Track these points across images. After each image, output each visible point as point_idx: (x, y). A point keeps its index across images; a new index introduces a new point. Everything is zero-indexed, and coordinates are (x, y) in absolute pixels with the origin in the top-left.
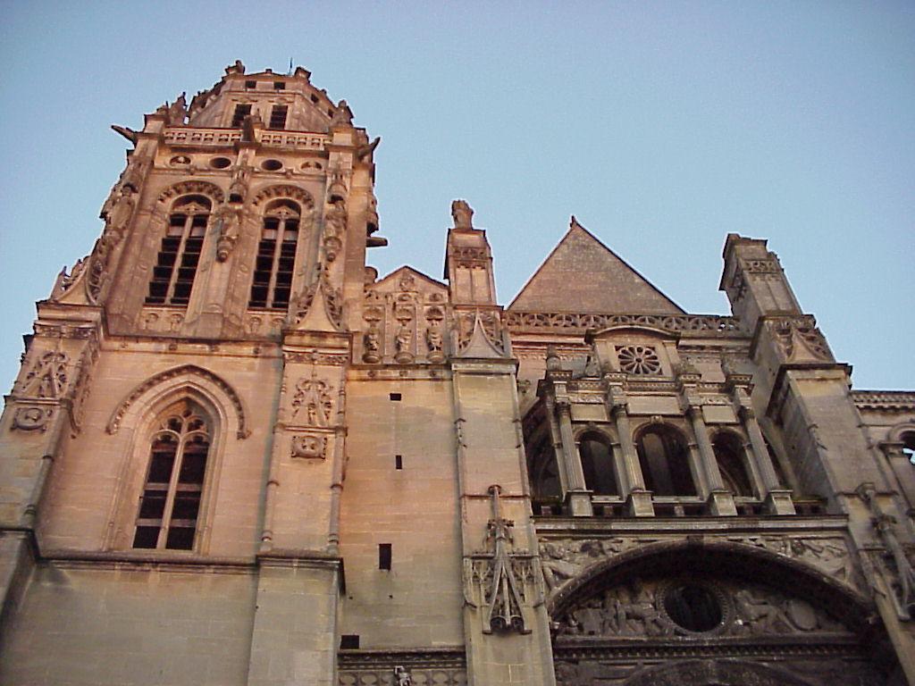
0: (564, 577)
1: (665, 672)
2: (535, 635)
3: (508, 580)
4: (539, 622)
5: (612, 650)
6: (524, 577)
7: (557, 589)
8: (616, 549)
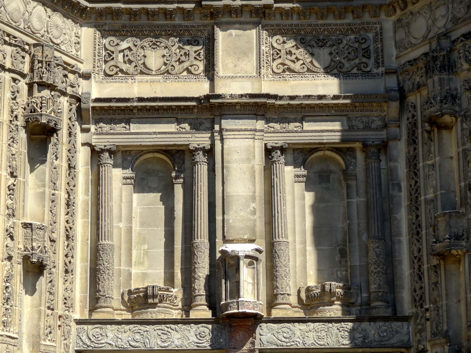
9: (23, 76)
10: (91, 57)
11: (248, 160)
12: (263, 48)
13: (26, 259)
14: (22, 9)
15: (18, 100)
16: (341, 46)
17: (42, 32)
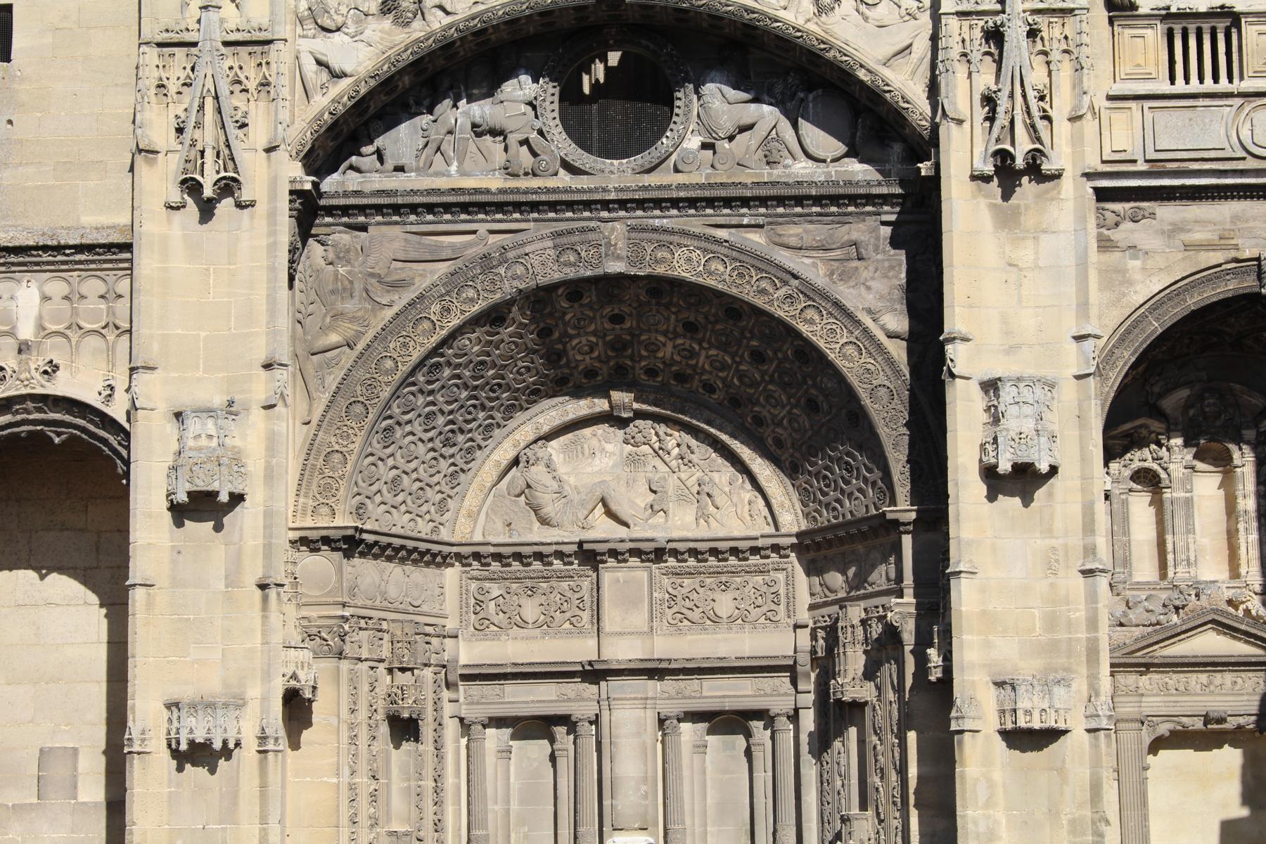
0: (337, 75)
1: (528, 249)
2: (261, 208)
3: (217, 98)
4: (273, 177)
5: (430, 208)
6: (252, 85)
7: (321, 102)
8: (449, 9)
10: (457, 610)
11: (639, 734)
12: (655, 595)
14: (377, 581)
15: (377, 690)
16: (746, 590)
17: (400, 599)
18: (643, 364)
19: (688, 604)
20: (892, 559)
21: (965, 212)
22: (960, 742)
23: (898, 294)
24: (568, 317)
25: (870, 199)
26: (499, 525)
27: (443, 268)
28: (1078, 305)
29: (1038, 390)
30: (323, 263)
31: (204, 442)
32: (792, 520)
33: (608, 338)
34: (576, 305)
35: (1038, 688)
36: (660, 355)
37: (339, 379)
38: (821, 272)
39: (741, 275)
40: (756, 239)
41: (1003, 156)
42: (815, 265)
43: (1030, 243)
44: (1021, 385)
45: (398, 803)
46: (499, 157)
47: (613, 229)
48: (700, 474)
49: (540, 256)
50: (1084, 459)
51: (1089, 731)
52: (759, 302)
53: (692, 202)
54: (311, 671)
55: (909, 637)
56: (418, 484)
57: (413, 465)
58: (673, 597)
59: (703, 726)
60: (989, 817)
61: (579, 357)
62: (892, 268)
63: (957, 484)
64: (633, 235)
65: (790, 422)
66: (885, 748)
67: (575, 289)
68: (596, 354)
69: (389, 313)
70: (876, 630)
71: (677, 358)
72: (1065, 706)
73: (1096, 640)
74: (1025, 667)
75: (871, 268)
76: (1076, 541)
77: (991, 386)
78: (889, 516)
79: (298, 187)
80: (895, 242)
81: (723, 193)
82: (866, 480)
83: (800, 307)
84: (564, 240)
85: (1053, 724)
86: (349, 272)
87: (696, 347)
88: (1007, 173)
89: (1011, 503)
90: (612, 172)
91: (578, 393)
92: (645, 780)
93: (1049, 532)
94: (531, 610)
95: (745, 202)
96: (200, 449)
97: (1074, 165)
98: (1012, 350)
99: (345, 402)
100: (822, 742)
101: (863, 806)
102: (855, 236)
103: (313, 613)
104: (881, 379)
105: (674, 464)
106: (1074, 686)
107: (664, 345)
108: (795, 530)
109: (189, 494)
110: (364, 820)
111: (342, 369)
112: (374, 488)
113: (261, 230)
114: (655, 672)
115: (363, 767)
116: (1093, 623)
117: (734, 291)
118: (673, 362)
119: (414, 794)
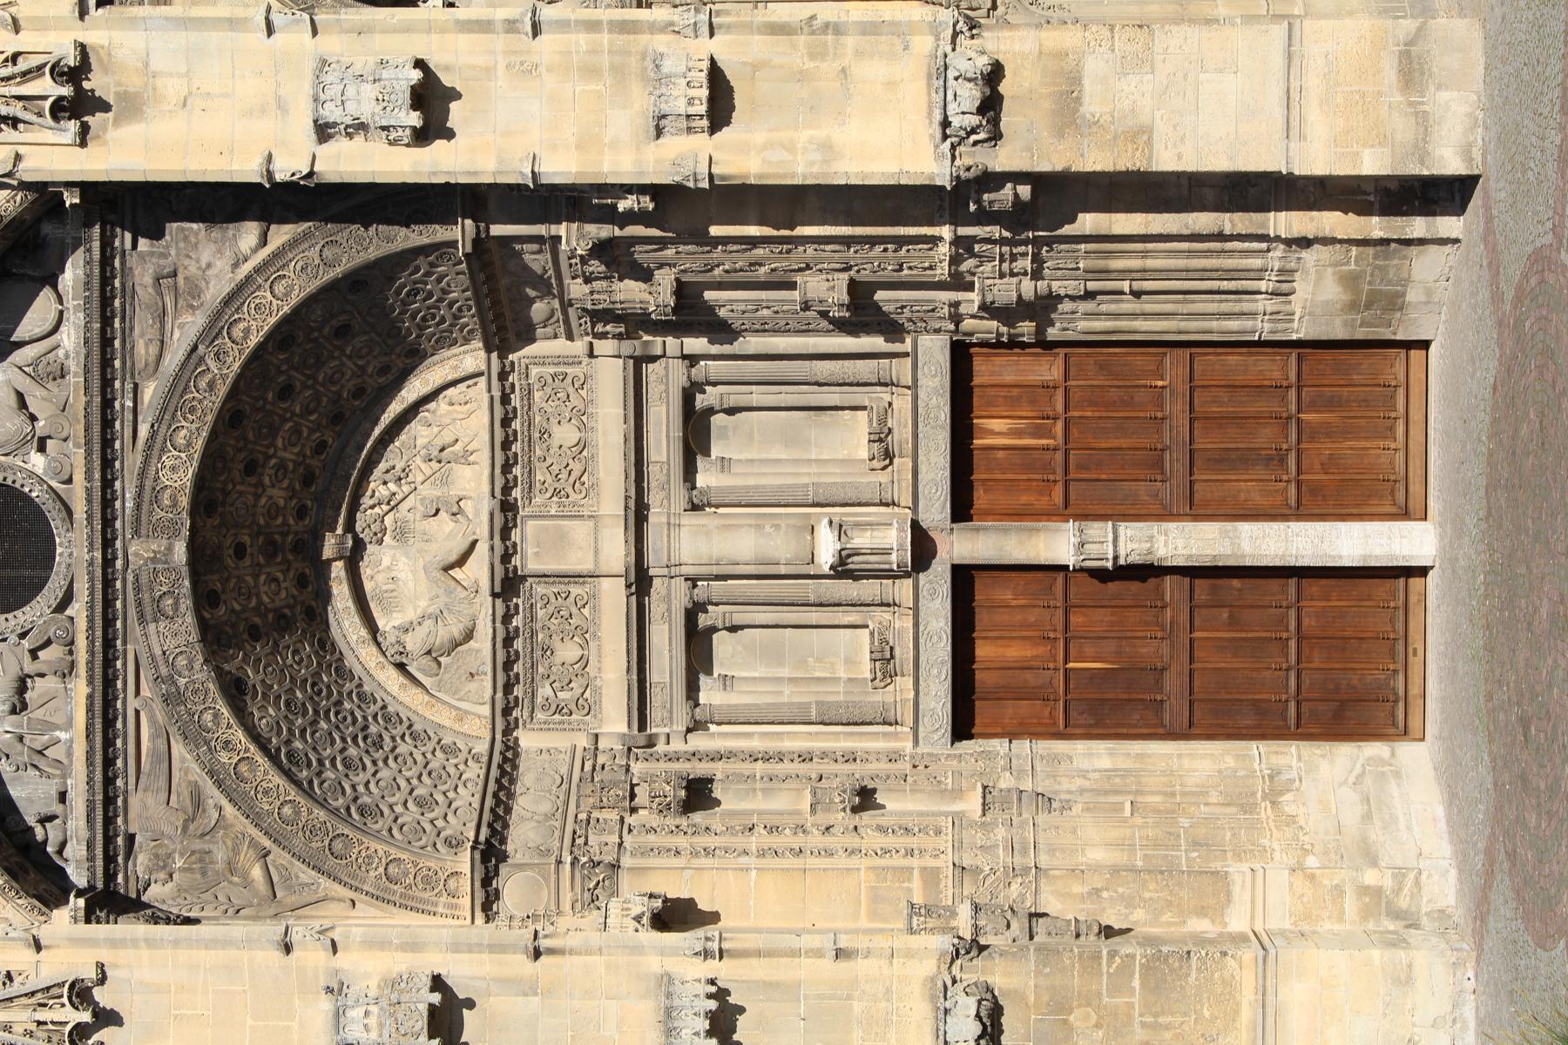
1: (158, 652)
2: (105, 956)
4: (69, 943)
5: (108, 762)
9: (622, 820)
11: (708, 534)
12: (553, 512)
13: (855, 810)
14: (533, 824)
16: (549, 410)
18: (291, 522)
19: (563, 476)
20: (518, 247)
21: (122, 154)
22: (723, 178)
23: (216, 233)
24: (237, 607)
25: (106, 261)
26: (472, 686)
27: (178, 749)
28: (232, 30)
29: (328, 79)
30: (170, 885)
31: (372, 1021)
32: (471, 357)
33: (262, 561)
34: (223, 597)
35: (664, 90)
36: (281, 502)
37: (304, 867)
38: (190, 319)
39: (192, 410)
40: (150, 392)
41: (60, 110)
42: (181, 326)
43: (160, 82)
44: (322, 97)
45: (780, 802)
46: (50, 683)
47: (136, 554)
48: (418, 460)
49: (167, 638)
50: (407, 29)
51: (712, 35)
52: (223, 390)
53: (107, 464)
54: (632, 899)
55: (606, 231)
56: (425, 778)
57: (403, 783)
58: (556, 492)
59: (701, 462)
60: (805, 149)
61: (283, 594)
62: (186, 238)
63: (434, 173)
64: (143, 532)
65: (361, 358)
66: (727, 262)
67: (204, 599)
68: (280, 575)
69: (229, 810)
70: (596, 266)
71: (285, 483)
72: (685, 59)
73: (611, 22)
74: (640, 103)
75: (186, 262)
76: (500, 41)
77: (324, 131)
78: (469, 249)
79: (82, 913)
80: (157, 234)
81: (97, 429)
82: (428, 274)
83: (230, 344)
84: (148, 610)
85: (704, 74)
86: (182, 855)
87: (273, 461)
88: (79, 105)
89: (457, 113)
90: (71, 554)
91: (325, 596)
92: (759, 527)
93: (489, 71)
94: (568, 652)
95: (107, 404)
96: (381, 1025)
97: (69, 29)
98: (281, 106)
99: (329, 860)
100: (721, 330)
101: (791, 286)
102: (148, 280)
103: (567, 897)
104: (314, 253)
105: (406, 489)
106: (661, 49)
107: (270, 498)
108: (482, 354)
109: (431, 1037)
110: (797, 841)
111: (292, 864)
112: (428, 827)
113: (132, 958)
114: (639, 515)
115: (740, 841)
116: (592, 26)
117: (210, 418)
118: (291, 488)
119: (770, 785)
